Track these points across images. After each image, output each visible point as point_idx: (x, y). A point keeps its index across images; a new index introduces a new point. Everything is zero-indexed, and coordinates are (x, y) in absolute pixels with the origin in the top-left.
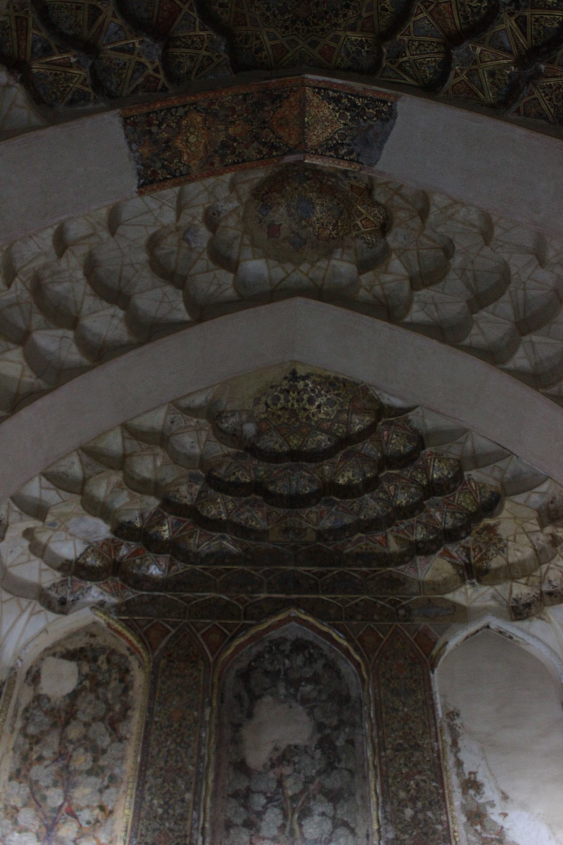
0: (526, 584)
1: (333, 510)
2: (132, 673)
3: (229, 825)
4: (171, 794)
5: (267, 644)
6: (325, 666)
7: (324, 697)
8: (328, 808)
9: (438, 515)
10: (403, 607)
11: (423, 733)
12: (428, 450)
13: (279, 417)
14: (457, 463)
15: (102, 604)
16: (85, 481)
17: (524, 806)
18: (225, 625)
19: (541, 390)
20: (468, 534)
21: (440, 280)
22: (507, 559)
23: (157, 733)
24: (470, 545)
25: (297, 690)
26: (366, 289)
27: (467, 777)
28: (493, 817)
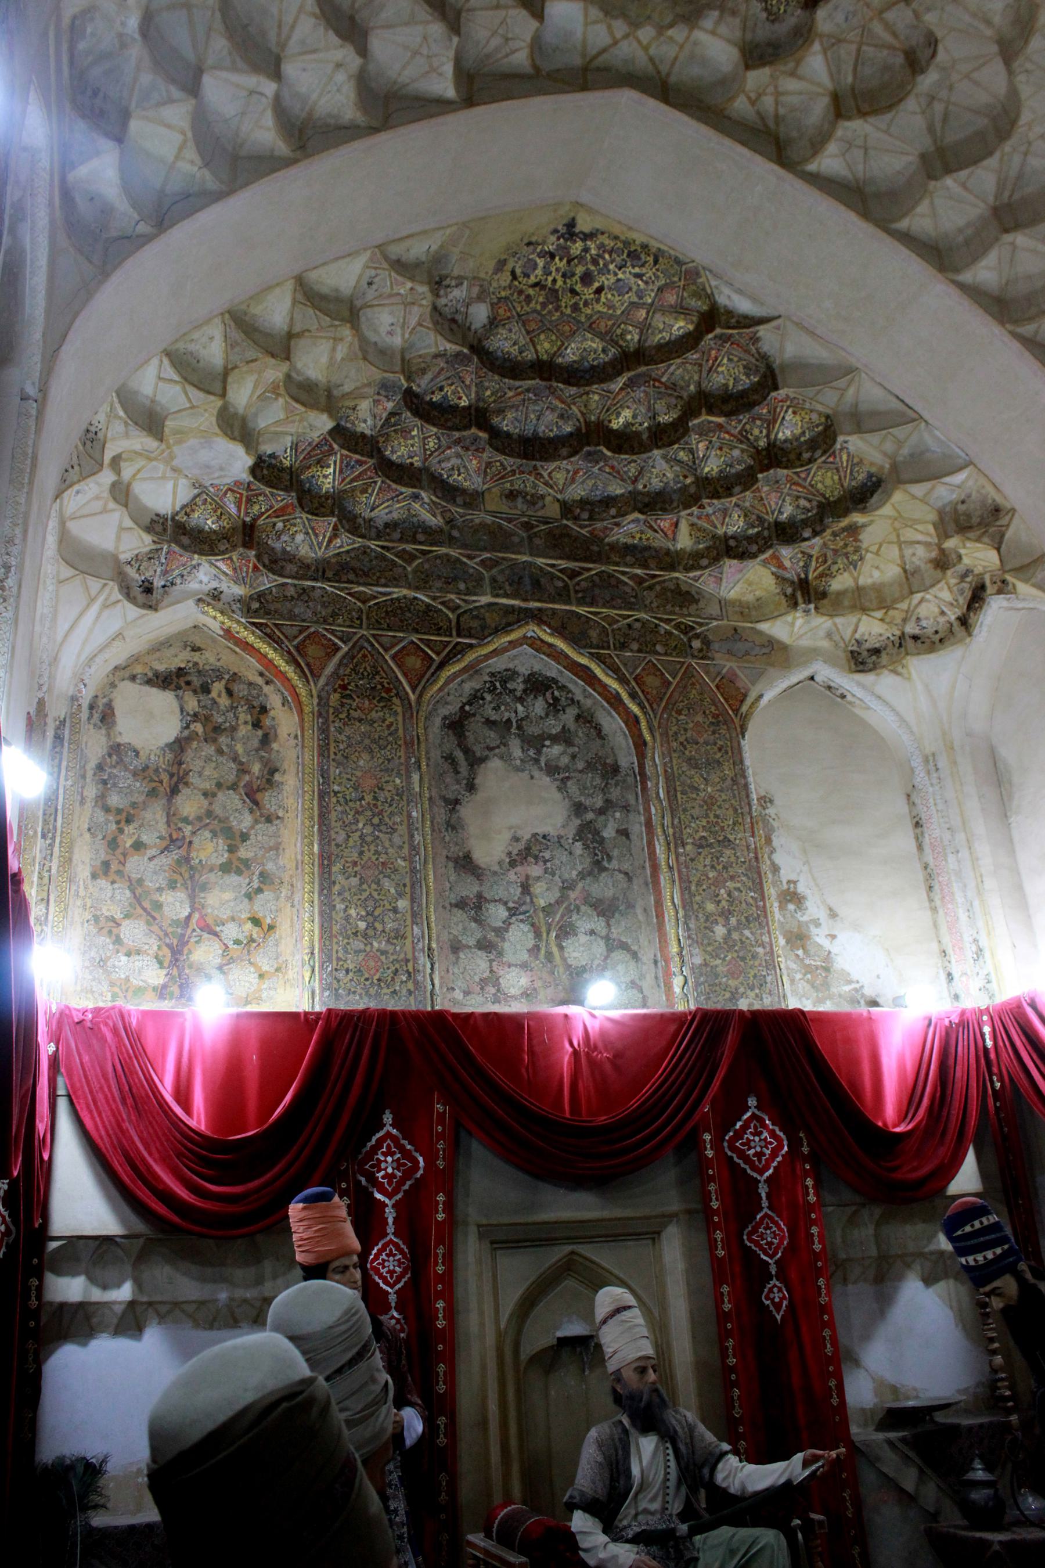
0: (882, 620)
1: (596, 470)
2: (272, 713)
3: (456, 948)
4: (376, 901)
5: (487, 678)
6: (578, 717)
7: (581, 765)
9: (773, 500)
10: (697, 636)
11: (734, 824)
12: (782, 393)
13: (529, 299)
14: (823, 420)
15: (216, 595)
16: (226, 373)
18: (428, 643)
19: (1008, 326)
20: (816, 534)
21: (890, 107)
22: (856, 580)
23: (339, 808)
24: (814, 552)
25: (539, 752)
26: (749, 98)
27: (785, 887)
28: (818, 940)
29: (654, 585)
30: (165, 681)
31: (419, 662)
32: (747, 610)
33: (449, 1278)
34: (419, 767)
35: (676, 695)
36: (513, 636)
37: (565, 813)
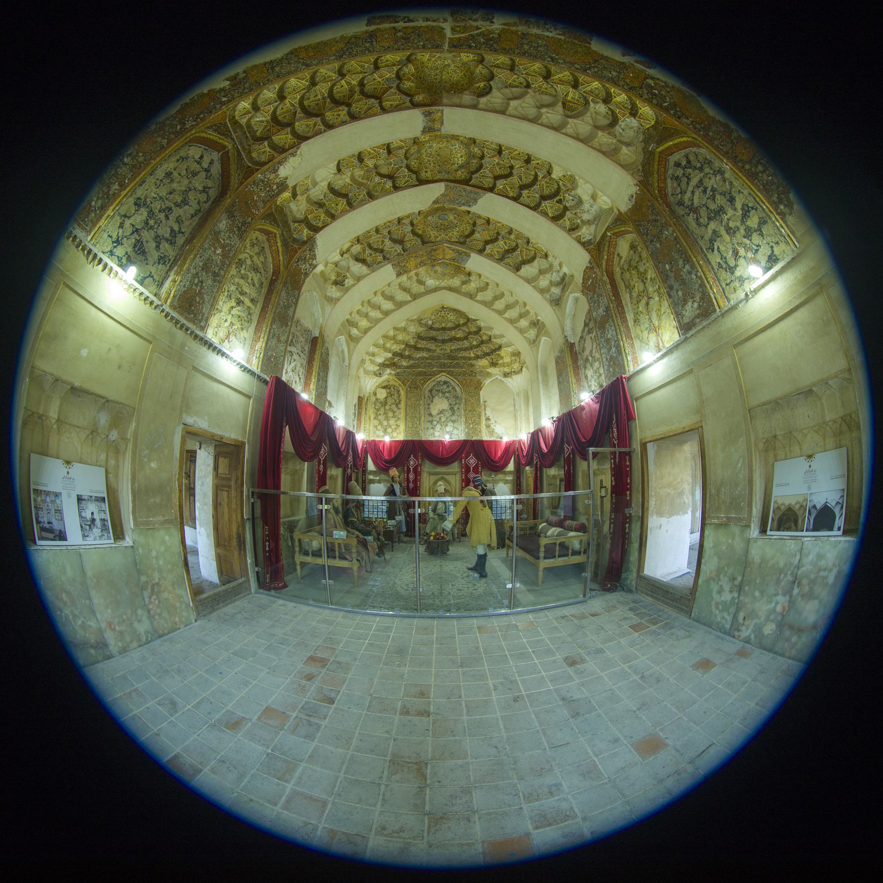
3: (428, 429)
8: (452, 424)
17: (500, 424)
30: (384, 387)
32: (483, 367)
33: (420, 479)
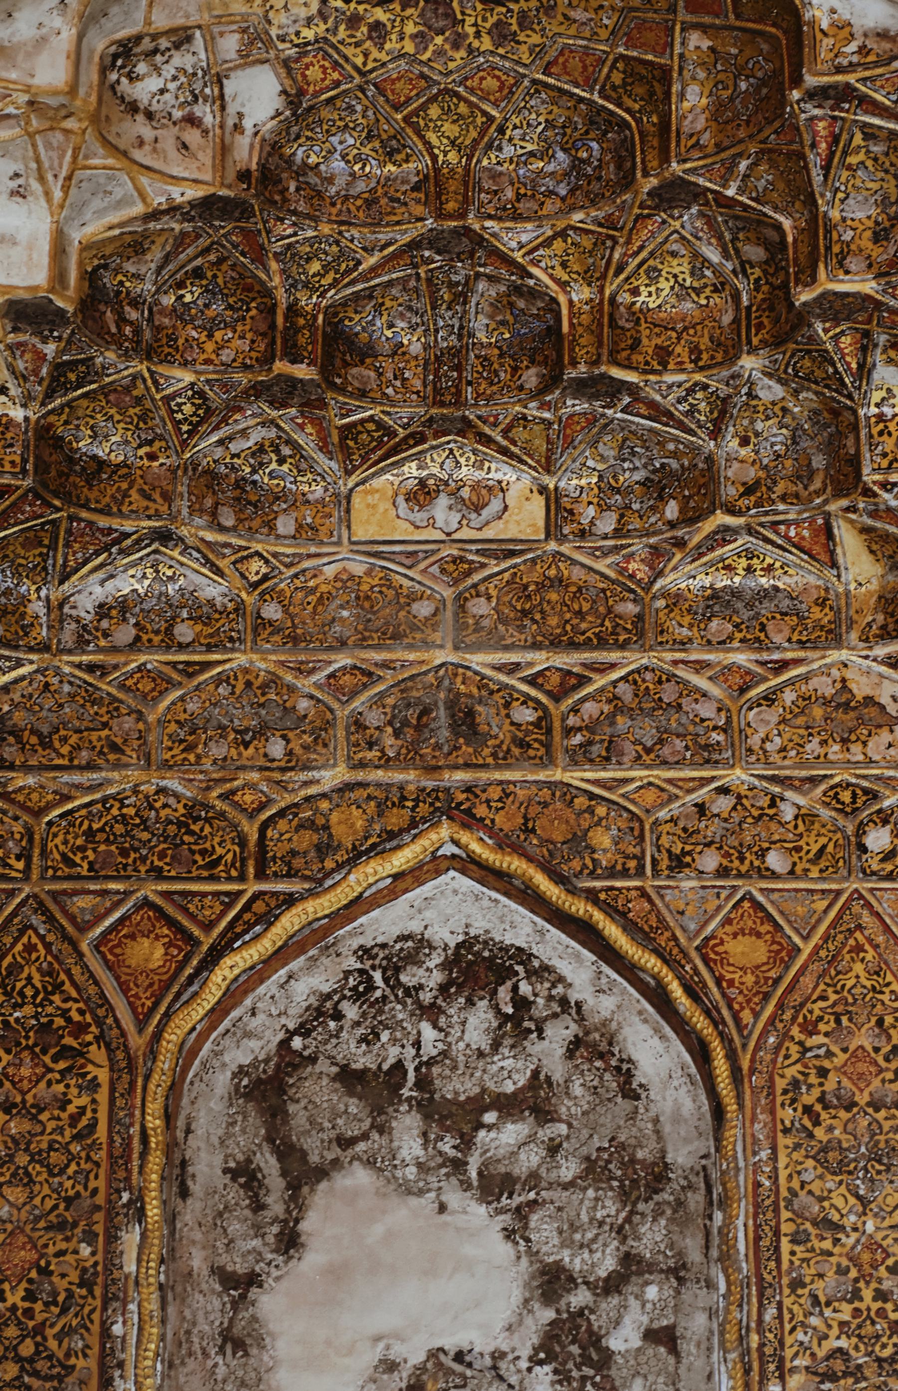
5: (352, 963)
6: (574, 1046)
7: (569, 1169)
25: (466, 1143)
29: (780, 688)
31: (159, 952)
34: (141, 1214)
35: (807, 981)
36: (400, 860)
37: (517, 1295)
